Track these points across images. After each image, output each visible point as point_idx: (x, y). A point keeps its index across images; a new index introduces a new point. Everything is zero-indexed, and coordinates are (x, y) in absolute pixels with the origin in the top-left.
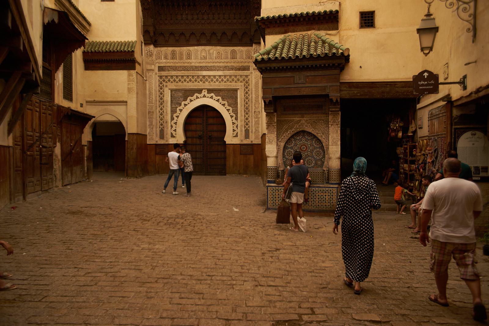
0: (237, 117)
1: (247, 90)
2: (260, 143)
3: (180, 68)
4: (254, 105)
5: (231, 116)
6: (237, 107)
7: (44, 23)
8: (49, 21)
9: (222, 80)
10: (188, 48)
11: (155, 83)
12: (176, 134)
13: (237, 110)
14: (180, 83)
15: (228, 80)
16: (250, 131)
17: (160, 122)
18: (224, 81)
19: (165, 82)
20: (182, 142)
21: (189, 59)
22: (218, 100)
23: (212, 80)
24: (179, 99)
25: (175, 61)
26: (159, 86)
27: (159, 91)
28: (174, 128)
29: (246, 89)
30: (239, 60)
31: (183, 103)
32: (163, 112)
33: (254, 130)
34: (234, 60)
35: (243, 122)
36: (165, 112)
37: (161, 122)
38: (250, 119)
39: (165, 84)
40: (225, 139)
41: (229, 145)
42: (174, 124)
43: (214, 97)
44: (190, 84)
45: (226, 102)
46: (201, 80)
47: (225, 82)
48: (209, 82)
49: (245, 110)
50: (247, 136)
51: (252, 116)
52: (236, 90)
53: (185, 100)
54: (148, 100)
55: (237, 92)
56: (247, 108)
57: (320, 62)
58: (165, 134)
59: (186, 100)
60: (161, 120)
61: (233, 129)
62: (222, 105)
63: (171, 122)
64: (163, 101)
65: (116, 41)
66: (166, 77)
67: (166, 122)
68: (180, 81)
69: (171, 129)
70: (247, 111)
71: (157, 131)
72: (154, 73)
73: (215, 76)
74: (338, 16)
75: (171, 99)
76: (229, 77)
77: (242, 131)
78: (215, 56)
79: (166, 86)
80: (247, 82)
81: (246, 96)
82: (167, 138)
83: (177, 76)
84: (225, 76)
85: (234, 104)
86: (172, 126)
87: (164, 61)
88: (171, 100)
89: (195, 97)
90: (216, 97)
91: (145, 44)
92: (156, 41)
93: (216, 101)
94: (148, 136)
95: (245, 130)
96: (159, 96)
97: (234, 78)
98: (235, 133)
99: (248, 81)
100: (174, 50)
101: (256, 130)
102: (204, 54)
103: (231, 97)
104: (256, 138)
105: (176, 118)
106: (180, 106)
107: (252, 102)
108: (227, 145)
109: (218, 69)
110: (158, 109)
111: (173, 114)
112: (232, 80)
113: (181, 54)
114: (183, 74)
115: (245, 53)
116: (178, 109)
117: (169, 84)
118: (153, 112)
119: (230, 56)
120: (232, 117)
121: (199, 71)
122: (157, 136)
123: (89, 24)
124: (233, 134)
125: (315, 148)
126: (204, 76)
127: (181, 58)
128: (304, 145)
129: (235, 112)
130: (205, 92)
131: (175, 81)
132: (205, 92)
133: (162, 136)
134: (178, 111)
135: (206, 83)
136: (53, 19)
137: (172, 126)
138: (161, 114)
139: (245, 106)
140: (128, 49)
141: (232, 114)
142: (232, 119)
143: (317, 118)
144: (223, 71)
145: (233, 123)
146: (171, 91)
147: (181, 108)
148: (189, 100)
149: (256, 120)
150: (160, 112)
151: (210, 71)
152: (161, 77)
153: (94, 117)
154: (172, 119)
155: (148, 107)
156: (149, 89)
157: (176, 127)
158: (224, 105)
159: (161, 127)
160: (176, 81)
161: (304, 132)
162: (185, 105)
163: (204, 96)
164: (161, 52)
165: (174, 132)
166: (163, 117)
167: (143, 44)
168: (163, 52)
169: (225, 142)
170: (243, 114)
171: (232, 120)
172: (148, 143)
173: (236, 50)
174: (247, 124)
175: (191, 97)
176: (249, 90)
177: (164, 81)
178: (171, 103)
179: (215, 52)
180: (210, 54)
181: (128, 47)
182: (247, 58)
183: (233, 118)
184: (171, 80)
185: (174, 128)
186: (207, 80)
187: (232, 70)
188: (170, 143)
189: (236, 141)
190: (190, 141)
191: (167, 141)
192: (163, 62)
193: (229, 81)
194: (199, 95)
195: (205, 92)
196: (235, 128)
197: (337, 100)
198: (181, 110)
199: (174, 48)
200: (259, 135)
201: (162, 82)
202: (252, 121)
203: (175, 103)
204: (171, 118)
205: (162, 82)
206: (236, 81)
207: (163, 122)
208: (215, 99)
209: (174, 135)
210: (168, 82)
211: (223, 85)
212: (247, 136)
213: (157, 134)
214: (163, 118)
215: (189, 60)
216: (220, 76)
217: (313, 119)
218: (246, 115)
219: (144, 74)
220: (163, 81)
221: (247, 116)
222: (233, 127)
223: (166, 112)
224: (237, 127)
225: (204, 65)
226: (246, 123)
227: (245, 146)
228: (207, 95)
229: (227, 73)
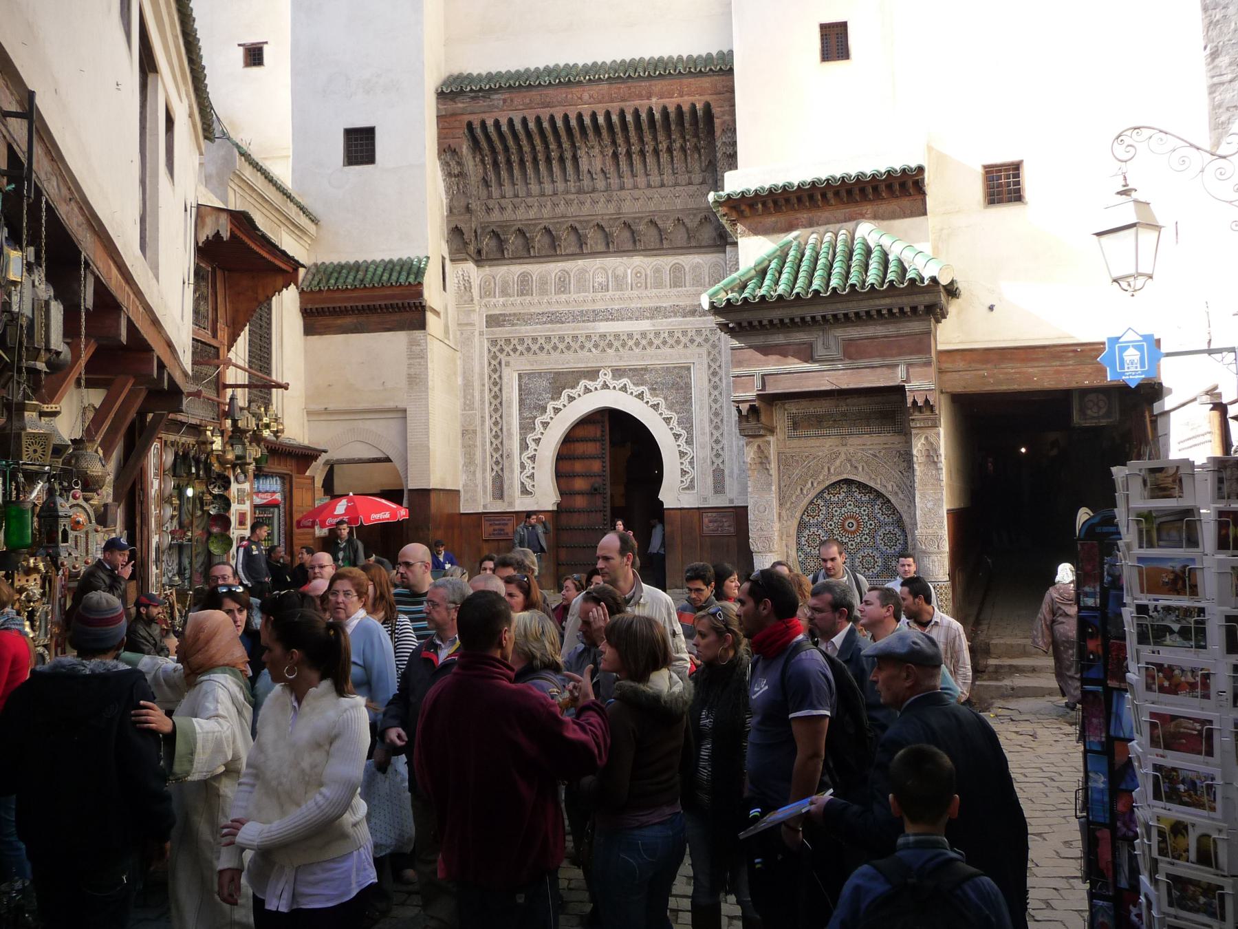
0: (692, 436)
3: (540, 317)
5: (674, 434)
6: (689, 411)
7: (197, 243)
8: (207, 237)
9: (651, 343)
10: (560, 264)
11: (481, 357)
14: (542, 356)
15: (664, 343)
16: (726, 472)
18: (655, 346)
19: (505, 353)
20: (550, 509)
21: (563, 292)
22: (640, 396)
23: (624, 345)
24: (540, 394)
25: (528, 298)
26: (490, 364)
27: (490, 377)
28: (528, 472)
29: (712, 364)
31: (551, 406)
32: (501, 429)
33: (736, 471)
35: (709, 448)
36: (504, 429)
37: (495, 455)
38: (725, 442)
39: (502, 356)
40: (661, 497)
41: (672, 512)
42: (529, 461)
43: (631, 387)
44: (569, 355)
45: (660, 400)
46: (596, 346)
47: (658, 347)
48: (617, 350)
50: (719, 487)
53: (556, 395)
56: (716, 414)
57: (877, 302)
59: (559, 398)
61: (682, 469)
62: (651, 406)
63: (521, 454)
64: (501, 403)
65: (378, 259)
66: (508, 341)
68: (542, 349)
69: (521, 473)
70: (716, 421)
71: (484, 478)
72: (477, 333)
74: (923, 179)
75: (520, 395)
76: (666, 335)
78: (629, 281)
79: (508, 364)
80: (714, 346)
81: (712, 382)
82: (511, 496)
83: (535, 340)
85: (683, 404)
86: (523, 466)
87: (501, 300)
88: (521, 401)
90: (636, 389)
91: (452, 260)
92: (479, 252)
93: (636, 396)
94: (462, 494)
96: (490, 390)
98: (687, 478)
100: (523, 273)
102: (600, 279)
103: (673, 385)
105: (532, 445)
106: (542, 415)
109: (637, 314)
110: (488, 423)
111: (526, 434)
113: (543, 282)
114: (547, 331)
115: (707, 271)
116: (538, 421)
117: (514, 358)
118: (475, 432)
120: (677, 436)
121: (589, 321)
122: (485, 492)
123: (314, 221)
124: (682, 482)
125: (881, 525)
126: (603, 336)
127: (543, 292)
128: (852, 517)
129: (687, 423)
131: (529, 349)
132: (606, 376)
133: (499, 491)
135: (609, 351)
136: (218, 231)
140: (407, 278)
141: (679, 430)
143: (882, 446)
144: (652, 318)
145: (682, 454)
146: (520, 375)
147: (545, 418)
148: (566, 398)
150: (491, 430)
151: (618, 320)
152: (494, 342)
153: (325, 452)
154: (524, 446)
156: (464, 373)
157: (533, 468)
158: (655, 407)
159: (495, 468)
160: (532, 351)
161: (848, 482)
162: (557, 410)
163: (605, 386)
164: (494, 278)
165: (528, 480)
166: (502, 443)
167: (447, 262)
168: (497, 279)
169: (662, 503)
170: (707, 430)
171: (679, 446)
172: (462, 512)
174: (718, 456)
175: (570, 390)
177: (501, 350)
178: (520, 406)
179: (629, 271)
180: (616, 277)
181: (408, 274)
183: (682, 441)
185: (528, 472)
186: (610, 345)
187: (675, 316)
189: (688, 501)
191: (511, 504)
192: (498, 305)
193: (668, 345)
194: (590, 384)
195: (605, 374)
196: (687, 467)
197: (927, 401)
198: (545, 425)
199: (526, 266)
201: (498, 354)
202: (731, 447)
203: (532, 407)
204: (521, 444)
205: (498, 354)
206: (685, 344)
207: (502, 456)
208: (632, 393)
210: (511, 353)
213: (485, 487)
214: (499, 446)
215: (563, 297)
216: (644, 334)
217: (870, 449)
218: (714, 432)
219: (451, 337)
220: (499, 351)
221: (716, 434)
222: (682, 463)
223: (509, 430)
224: (691, 463)
225: (599, 306)
226: (715, 452)
227: (714, 514)
228: (612, 382)
229: (663, 324)
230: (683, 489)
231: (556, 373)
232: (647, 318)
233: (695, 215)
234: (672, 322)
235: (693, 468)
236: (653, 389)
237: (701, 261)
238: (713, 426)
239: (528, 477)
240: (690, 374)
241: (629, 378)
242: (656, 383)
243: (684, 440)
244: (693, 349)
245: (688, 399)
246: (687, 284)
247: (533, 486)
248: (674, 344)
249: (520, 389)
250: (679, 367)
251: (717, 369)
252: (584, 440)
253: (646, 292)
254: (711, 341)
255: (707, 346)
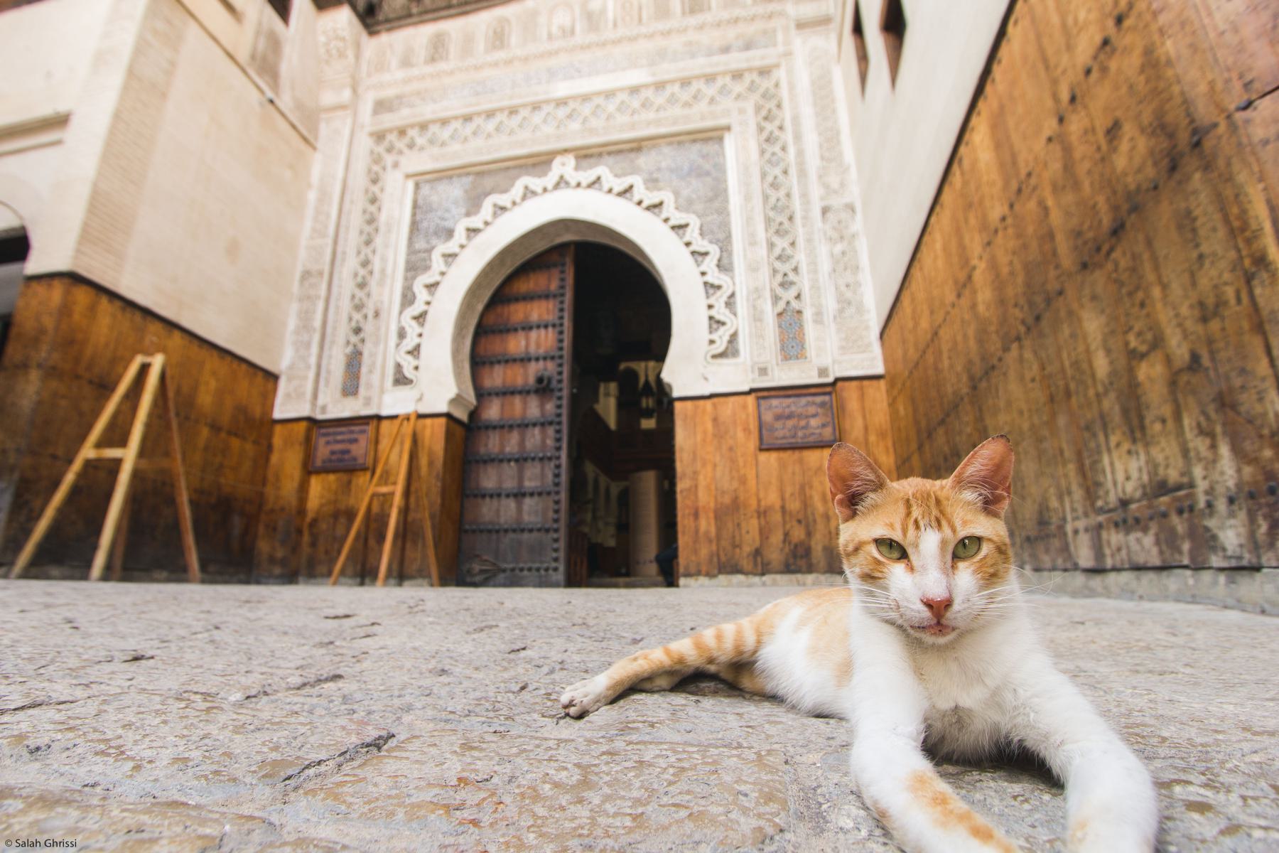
1: (769, 127)
2: (880, 369)
4: (820, 177)
6: (723, 211)
12: (416, 368)
13: (725, 226)
14: (456, 147)
16: (808, 314)
17: (350, 319)
20: (443, 408)
30: (725, 15)
32: (371, 273)
33: (830, 304)
35: (765, 272)
38: (801, 257)
39: (389, 159)
41: (689, 404)
43: (609, 180)
45: (667, 196)
49: (772, 214)
50: (792, 345)
51: (809, 240)
52: (713, 135)
53: (474, 206)
54: (308, 224)
55: (722, 147)
58: (364, 370)
60: (359, 307)
63: (401, 313)
67: (377, 314)
69: (398, 345)
70: (779, 219)
73: (609, 94)
75: (414, 215)
77: (760, 320)
80: (765, 96)
81: (767, 156)
82: (369, 386)
84: (660, 86)
85: (711, 200)
86: (402, 334)
89: (517, 190)
90: (618, 181)
95: (780, 315)
101: (844, 303)
104: (850, 343)
105: (422, 295)
107: (802, 173)
108: (678, 405)
111: (414, 278)
120: (699, 255)
124: (712, 342)
126: (562, 102)
130: (564, 167)
132: (564, 167)
134: (437, 263)
137: (402, 334)
138: (362, 286)
139: (766, 198)
142: (703, 268)
145: (711, 288)
147: (452, 246)
149: (839, 248)
152: (379, 136)
154: (408, 298)
155: (302, 254)
162: (473, 231)
163: (561, 183)
170: (761, 234)
176: (781, 128)
177: (390, 150)
183: (710, 264)
184: (420, 141)
185: (409, 343)
188: (384, 413)
190: (493, 412)
191: (368, 401)
194: (535, 183)
196: (721, 312)
198: (450, 257)
200: (867, 328)
204: (404, 296)
209: (408, 372)
210: (406, 150)
211: (649, 123)
212: (792, 345)
215: (501, 55)
216: (634, 90)
218: (776, 239)
221: (781, 244)
222: (710, 307)
223: (383, 271)
224: (730, 303)
226: (779, 278)
228: (574, 174)
230: (714, 357)
231: (479, 174)
235: (735, 314)
236: (652, 183)
238: (772, 231)
239: (409, 353)
241: (607, 165)
242: (659, 170)
243: (715, 262)
244: (727, 103)
245: (718, 194)
247: (416, 368)
249: (415, 206)
251: (777, 133)
252: (529, 297)
254: (762, 90)
255: (756, 97)
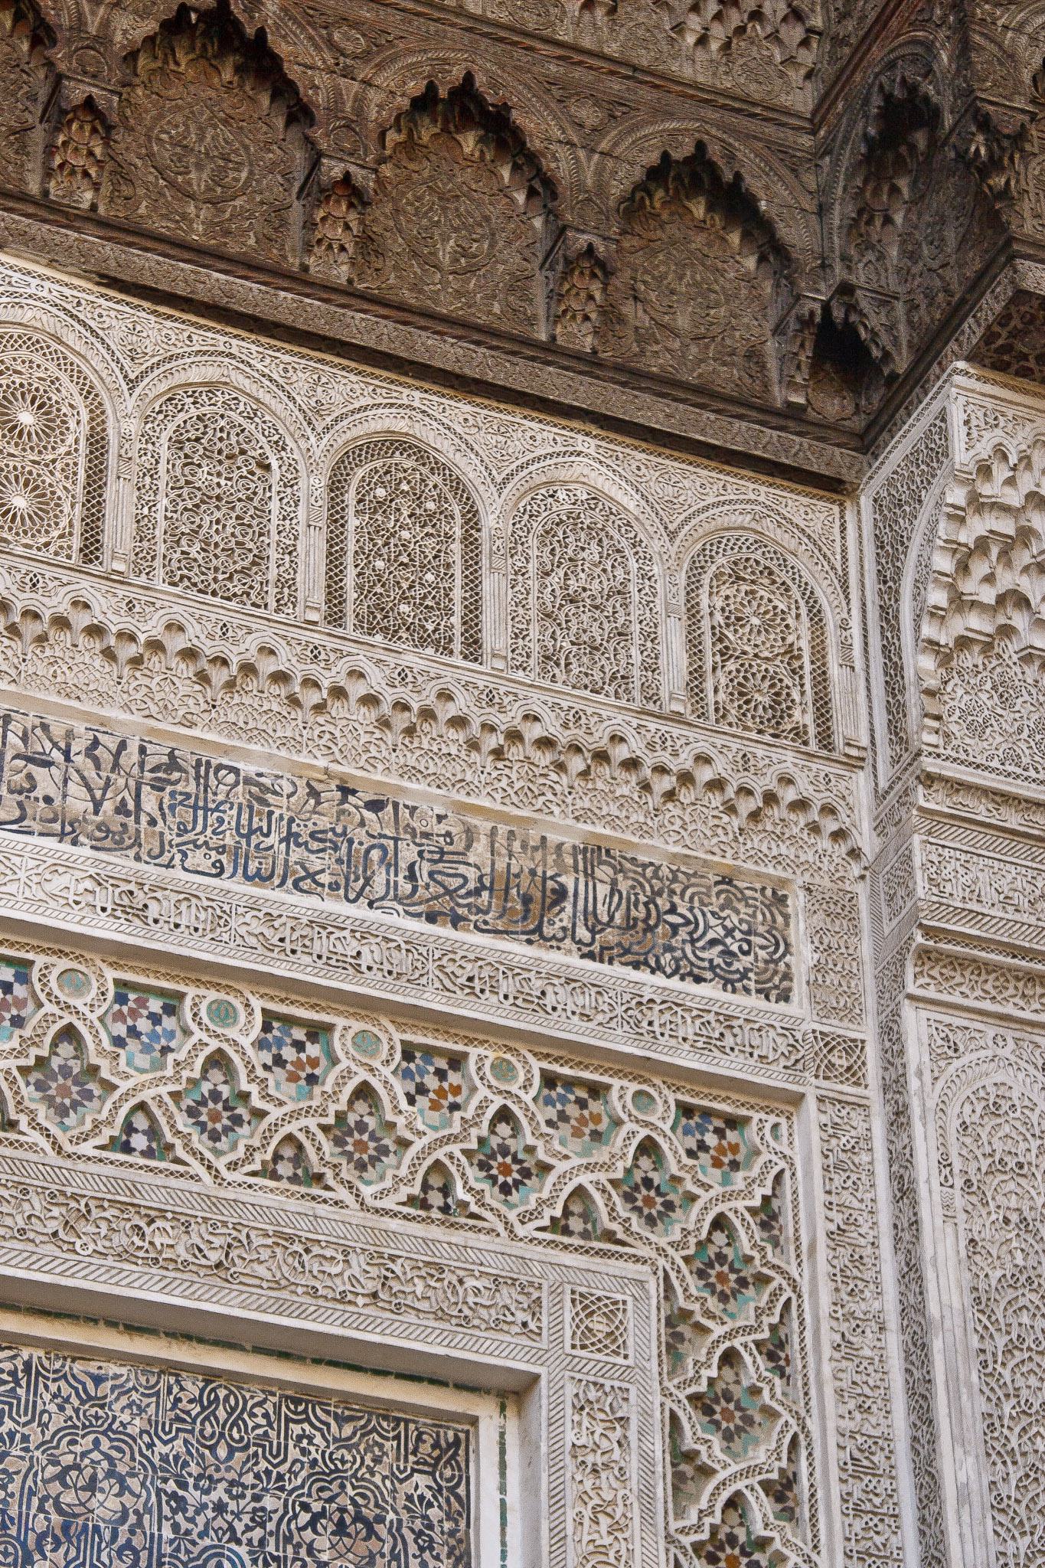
34: (414, 659)
97: (391, 1087)
99: (747, 1238)
112: (339, 1130)
115: (669, 587)
119: (312, 549)
144: (109, 839)
173: (468, 469)
182: (717, 687)
232: (69, 831)
233: (615, 109)
234: (323, 925)
237: (630, 502)
240: (461, 1509)
246: (494, 635)
248: (322, 1152)
250: (349, 1407)
251: (761, 1509)
253: (85, 587)
254: (694, 1220)
